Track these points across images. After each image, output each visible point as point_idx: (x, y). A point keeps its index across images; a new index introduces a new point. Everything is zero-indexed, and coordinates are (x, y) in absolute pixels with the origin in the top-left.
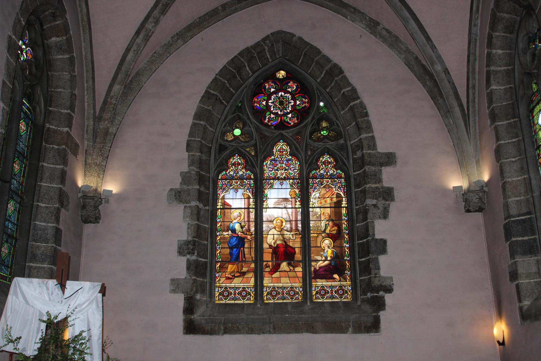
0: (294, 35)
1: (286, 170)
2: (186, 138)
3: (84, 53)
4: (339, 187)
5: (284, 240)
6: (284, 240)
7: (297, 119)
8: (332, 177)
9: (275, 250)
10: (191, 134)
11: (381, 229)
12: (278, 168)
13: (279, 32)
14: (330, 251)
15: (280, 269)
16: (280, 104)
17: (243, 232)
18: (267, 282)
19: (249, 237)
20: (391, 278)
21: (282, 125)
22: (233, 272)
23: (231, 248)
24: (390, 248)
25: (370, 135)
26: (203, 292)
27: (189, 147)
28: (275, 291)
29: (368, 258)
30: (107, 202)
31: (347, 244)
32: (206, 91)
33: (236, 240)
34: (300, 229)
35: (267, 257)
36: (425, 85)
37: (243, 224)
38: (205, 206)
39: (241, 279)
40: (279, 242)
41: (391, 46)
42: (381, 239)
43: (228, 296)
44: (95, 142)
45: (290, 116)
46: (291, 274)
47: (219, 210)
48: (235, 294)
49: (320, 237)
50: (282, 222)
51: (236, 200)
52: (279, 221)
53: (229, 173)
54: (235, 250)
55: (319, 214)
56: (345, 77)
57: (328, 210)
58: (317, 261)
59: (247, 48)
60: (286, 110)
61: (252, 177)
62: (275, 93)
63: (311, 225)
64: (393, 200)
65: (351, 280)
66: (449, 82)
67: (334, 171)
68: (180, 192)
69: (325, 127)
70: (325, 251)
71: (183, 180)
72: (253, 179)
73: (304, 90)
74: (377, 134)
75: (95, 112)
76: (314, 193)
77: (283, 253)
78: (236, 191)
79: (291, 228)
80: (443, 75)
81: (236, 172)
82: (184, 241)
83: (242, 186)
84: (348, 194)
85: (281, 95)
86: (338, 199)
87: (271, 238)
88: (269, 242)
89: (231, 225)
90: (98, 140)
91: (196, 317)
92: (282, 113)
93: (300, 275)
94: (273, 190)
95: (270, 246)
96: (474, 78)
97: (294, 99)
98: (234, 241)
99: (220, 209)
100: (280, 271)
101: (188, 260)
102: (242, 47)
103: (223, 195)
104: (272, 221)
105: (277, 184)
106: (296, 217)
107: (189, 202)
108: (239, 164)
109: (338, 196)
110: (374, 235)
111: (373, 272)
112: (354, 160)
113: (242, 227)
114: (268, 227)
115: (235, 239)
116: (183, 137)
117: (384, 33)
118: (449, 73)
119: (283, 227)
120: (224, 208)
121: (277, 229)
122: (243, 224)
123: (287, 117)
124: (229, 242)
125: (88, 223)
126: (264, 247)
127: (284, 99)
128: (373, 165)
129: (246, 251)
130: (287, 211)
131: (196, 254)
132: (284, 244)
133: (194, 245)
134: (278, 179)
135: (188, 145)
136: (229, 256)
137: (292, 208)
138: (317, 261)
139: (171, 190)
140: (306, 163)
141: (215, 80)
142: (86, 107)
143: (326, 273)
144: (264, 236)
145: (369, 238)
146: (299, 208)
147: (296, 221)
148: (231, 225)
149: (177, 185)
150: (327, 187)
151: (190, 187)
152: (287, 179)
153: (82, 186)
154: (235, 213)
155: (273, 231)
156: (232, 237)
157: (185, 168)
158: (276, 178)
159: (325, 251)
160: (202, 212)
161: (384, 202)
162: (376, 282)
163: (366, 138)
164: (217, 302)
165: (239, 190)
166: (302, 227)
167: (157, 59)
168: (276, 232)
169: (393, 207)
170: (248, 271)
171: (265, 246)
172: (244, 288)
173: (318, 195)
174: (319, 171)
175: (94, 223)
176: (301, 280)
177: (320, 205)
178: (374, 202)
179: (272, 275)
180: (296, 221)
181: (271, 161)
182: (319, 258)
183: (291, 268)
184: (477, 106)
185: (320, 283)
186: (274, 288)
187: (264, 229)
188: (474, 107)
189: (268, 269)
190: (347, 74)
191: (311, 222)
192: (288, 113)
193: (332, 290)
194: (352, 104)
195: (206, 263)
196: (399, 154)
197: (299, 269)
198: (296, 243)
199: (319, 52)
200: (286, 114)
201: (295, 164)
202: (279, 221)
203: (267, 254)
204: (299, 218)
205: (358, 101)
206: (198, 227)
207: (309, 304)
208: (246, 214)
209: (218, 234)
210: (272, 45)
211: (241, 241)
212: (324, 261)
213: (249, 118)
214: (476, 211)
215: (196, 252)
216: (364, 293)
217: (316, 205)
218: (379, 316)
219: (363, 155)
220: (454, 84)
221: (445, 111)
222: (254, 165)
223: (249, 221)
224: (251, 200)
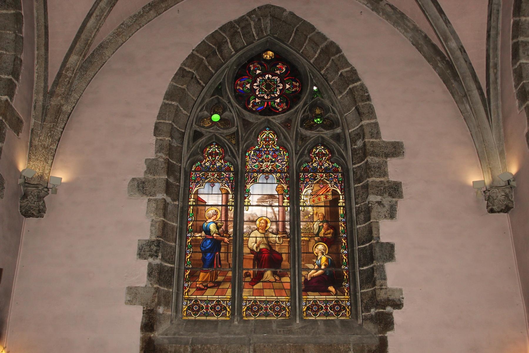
0: (285, 10)
1: (272, 162)
2: (154, 120)
3: (35, 14)
4: (335, 183)
5: (269, 244)
6: (269, 244)
7: (287, 105)
8: (327, 171)
10: (160, 116)
11: (387, 231)
12: (263, 159)
13: (267, 6)
14: (324, 258)
15: (264, 279)
17: (219, 234)
18: (246, 294)
19: (226, 240)
20: (401, 290)
22: (206, 281)
23: (204, 252)
25: (373, 121)
26: (167, 304)
27: (157, 130)
28: (256, 305)
29: (372, 265)
30: (55, 192)
31: (345, 250)
32: (180, 68)
33: (210, 243)
34: (288, 231)
36: (435, 67)
37: (219, 224)
38: (174, 200)
39: (215, 290)
40: (262, 247)
41: (395, 23)
42: (388, 243)
43: (198, 311)
44: (44, 120)
45: (278, 101)
46: (277, 285)
47: (192, 207)
48: (207, 309)
49: (313, 241)
50: (267, 223)
51: (212, 196)
52: (263, 221)
53: (204, 164)
54: (209, 254)
55: (311, 213)
56: (343, 56)
57: (322, 210)
58: (309, 270)
59: (230, 23)
60: (274, 94)
61: (232, 169)
62: (262, 75)
63: (302, 227)
64: (401, 197)
65: (349, 293)
66: (466, 62)
67: (329, 164)
68: (144, 183)
69: (319, 115)
70: (319, 258)
71: (148, 167)
72: (232, 172)
74: (380, 120)
75: (46, 87)
76: (305, 190)
77: (267, 258)
78: (213, 185)
79: (278, 230)
80: (458, 53)
81: (213, 163)
82: (146, 240)
83: (219, 179)
84: (346, 190)
85: (268, 78)
86: (334, 197)
87: (254, 241)
88: (250, 246)
89: (205, 225)
90: (48, 118)
91: (157, 335)
92: (269, 98)
93: (287, 286)
94: (256, 186)
95: (252, 251)
96: (496, 56)
99: (193, 205)
100: (262, 282)
101: (150, 264)
102: (224, 22)
103: (196, 189)
104: (254, 222)
105: (261, 177)
106: (284, 217)
107: (155, 195)
108: (217, 154)
109: (334, 193)
110: (379, 237)
111: (378, 282)
112: (354, 151)
113: (218, 228)
114: (250, 228)
115: (209, 242)
116: (151, 119)
117: (389, 9)
118: (465, 51)
119: (267, 228)
120: (197, 205)
121: (260, 230)
122: (219, 224)
123: (275, 102)
124: (202, 246)
125: (29, 216)
126: (244, 252)
127: (271, 82)
128: (377, 156)
129: (222, 256)
130: (273, 209)
131: (160, 257)
132: (269, 248)
133: (158, 246)
134: (263, 172)
135: (156, 128)
136: (202, 262)
137: (279, 206)
138: (309, 270)
139: (133, 179)
140: (296, 154)
141: (191, 56)
142: (35, 79)
144: (245, 238)
145: (373, 242)
146: (287, 206)
147: (284, 221)
148: (205, 225)
149: (141, 173)
150: (321, 182)
151: (156, 177)
152: (274, 173)
153: (23, 171)
154: (211, 211)
155: (256, 233)
156: (205, 239)
157: (151, 154)
158: (260, 171)
160: (170, 208)
161: (390, 199)
162: (382, 295)
163: (368, 124)
164: (184, 318)
165: (216, 184)
166: (290, 229)
167: (125, 31)
168: (259, 235)
169: (402, 205)
170: (225, 281)
171: (246, 250)
172: (218, 301)
173: (310, 192)
174: (312, 164)
175: (37, 217)
176: (289, 293)
177: (312, 204)
178: (379, 198)
179: (253, 285)
180: (284, 221)
181: (255, 151)
182: (311, 266)
183: (277, 278)
184: (499, 88)
185: (312, 296)
186: (255, 301)
187: (245, 230)
188: (496, 89)
189: (248, 279)
190: (346, 53)
191: (302, 223)
192: (277, 98)
193: (326, 306)
194: (351, 86)
195: (172, 269)
196: (406, 144)
199: (313, 29)
202: (263, 221)
203: (247, 260)
204: (287, 218)
205: (358, 83)
206: (165, 225)
207: (298, 322)
208: (223, 212)
209: (189, 235)
210: (259, 19)
211: (217, 244)
212: (317, 270)
213: (230, 102)
214: (502, 211)
215: (160, 254)
216: (367, 309)
217: (308, 203)
218: (386, 337)
219: (365, 145)
220: (471, 64)
221: (460, 96)
223: (226, 221)
224: (230, 196)
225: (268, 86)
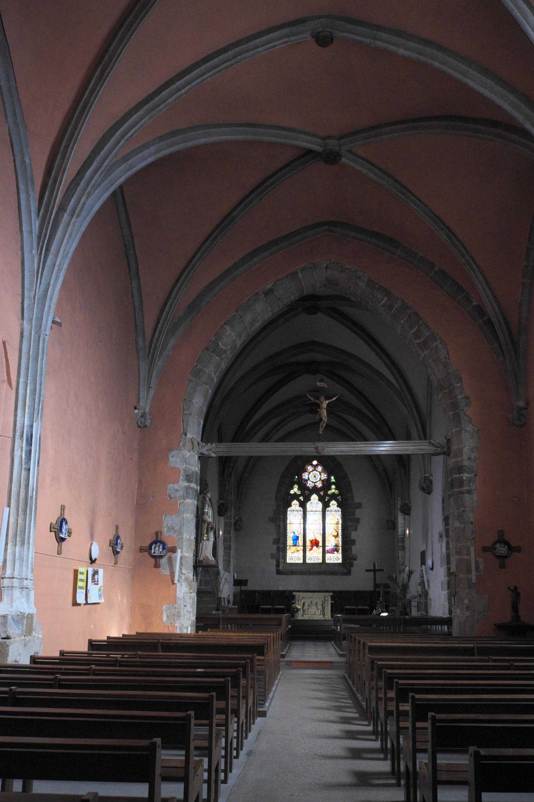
9: (311, 542)
11: (354, 535)
16: (314, 476)
24: (357, 543)
35: (308, 544)
46: (318, 551)
77: (315, 543)
97: (320, 475)
98: (295, 538)
135: (276, 498)
159: (331, 542)
169: (359, 527)
171: (307, 540)
197: (321, 549)
198: (320, 539)
200: (316, 482)
201: (320, 505)
222: (303, 505)
225: (315, 477)
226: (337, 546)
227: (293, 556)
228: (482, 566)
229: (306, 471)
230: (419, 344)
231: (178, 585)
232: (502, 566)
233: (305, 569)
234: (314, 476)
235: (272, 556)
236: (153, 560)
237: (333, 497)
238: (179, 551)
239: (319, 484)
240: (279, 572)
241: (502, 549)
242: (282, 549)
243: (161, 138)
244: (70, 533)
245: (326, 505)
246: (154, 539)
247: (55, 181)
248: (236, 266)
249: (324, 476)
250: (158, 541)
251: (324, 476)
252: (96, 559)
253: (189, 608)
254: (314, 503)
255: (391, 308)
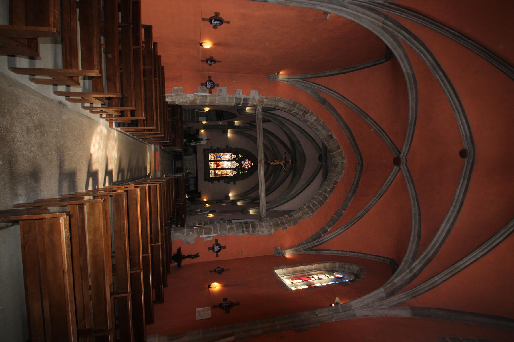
9: (219, 164)
11: (222, 182)
16: (247, 164)
21: (242, 165)
35: (217, 162)
73: (249, 168)
77: (218, 165)
143: (215, 173)
198: (220, 167)
222: (234, 160)
226: (217, 174)
227: (212, 156)
228: (208, 239)
229: (249, 160)
230: (309, 206)
231: (193, 95)
232: (209, 249)
233: (207, 161)
234: (247, 164)
235: (212, 147)
236: (204, 82)
237: (238, 172)
238: (210, 95)
239: (243, 166)
240: (205, 150)
241: (217, 248)
242: (214, 152)
243: (414, 76)
244: (215, 27)
245: (234, 169)
246: (215, 83)
247: (403, 12)
248: (343, 121)
249: (247, 168)
250: (214, 85)
251: (247, 168)
252: (202, 46)
253: (182, 100)
254: (235, 164)
255: (325, 192)
